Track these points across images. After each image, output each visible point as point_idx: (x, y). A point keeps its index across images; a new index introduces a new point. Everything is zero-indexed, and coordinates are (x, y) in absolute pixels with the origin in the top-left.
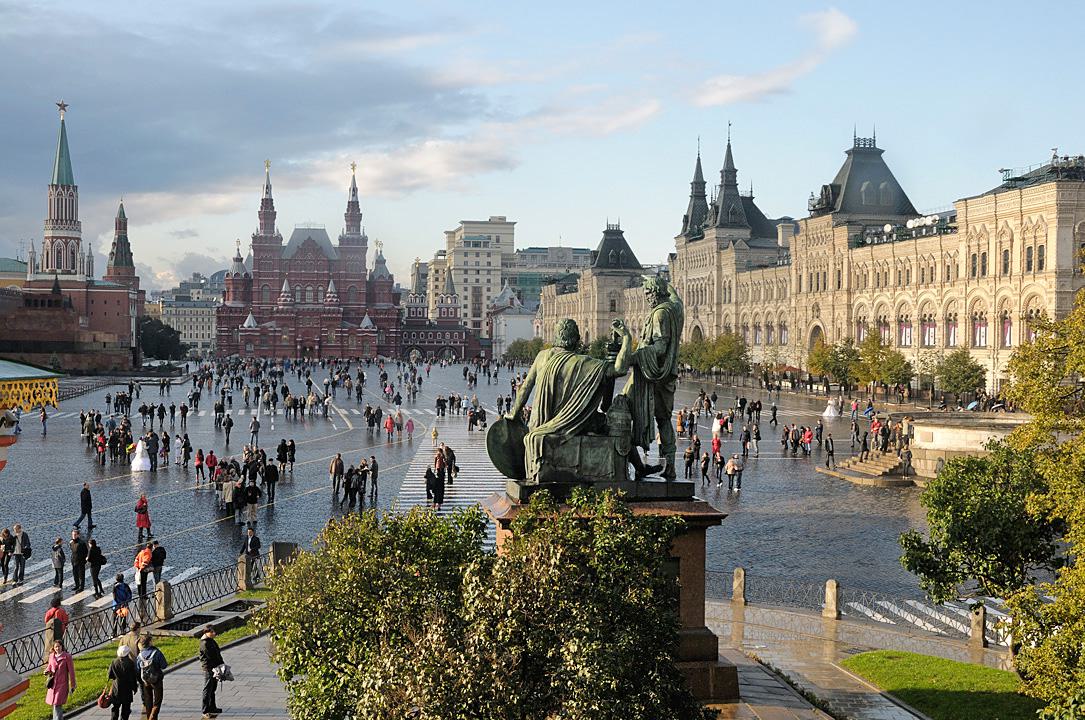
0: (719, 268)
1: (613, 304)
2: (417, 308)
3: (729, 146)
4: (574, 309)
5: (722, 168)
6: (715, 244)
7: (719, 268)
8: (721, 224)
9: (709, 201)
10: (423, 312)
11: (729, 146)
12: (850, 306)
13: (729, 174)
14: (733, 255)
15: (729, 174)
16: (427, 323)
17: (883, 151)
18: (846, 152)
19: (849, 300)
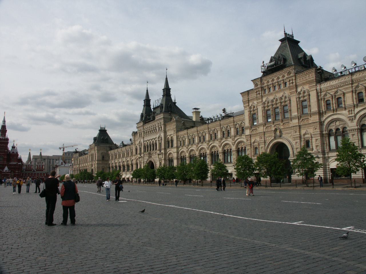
0: (165, 132)
1: (103, 157)
2: (29, 166)
3: (167, 79)
4: (86, 161)
5: (163, 88)
6: (163, 120)
7: (165, 132)
8: (165, 112)
9: (152, 107)
10: (31, 167)
11: (167, 79)
12: (321, 123)
13: (167, 91)
14: (175, 123)
15: (167, 91)
16: (33, 170)
17: (299, 42)
18: (280, 40)
19: (320, 119)
